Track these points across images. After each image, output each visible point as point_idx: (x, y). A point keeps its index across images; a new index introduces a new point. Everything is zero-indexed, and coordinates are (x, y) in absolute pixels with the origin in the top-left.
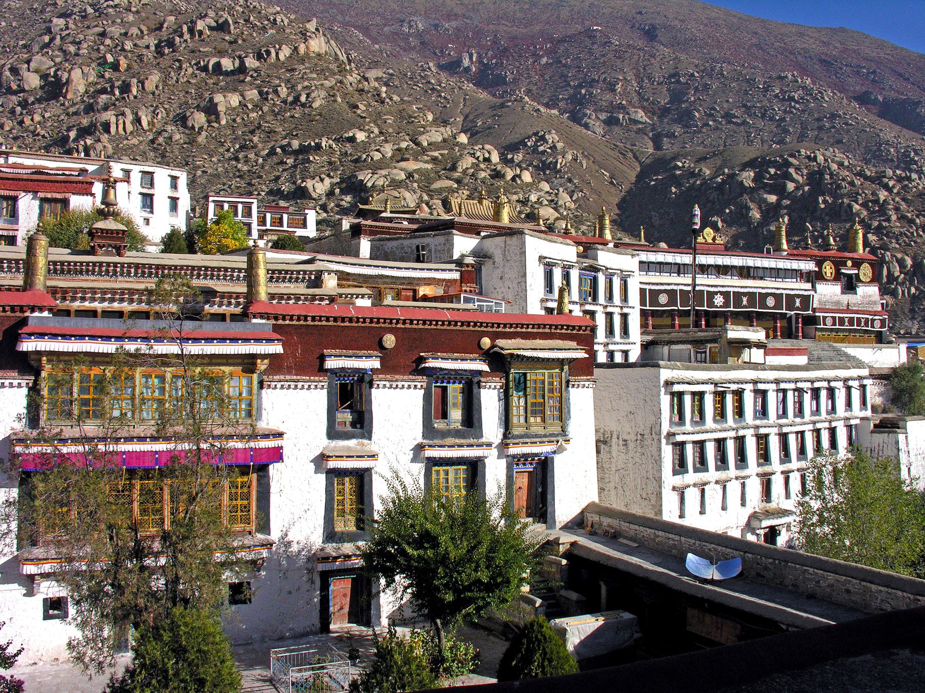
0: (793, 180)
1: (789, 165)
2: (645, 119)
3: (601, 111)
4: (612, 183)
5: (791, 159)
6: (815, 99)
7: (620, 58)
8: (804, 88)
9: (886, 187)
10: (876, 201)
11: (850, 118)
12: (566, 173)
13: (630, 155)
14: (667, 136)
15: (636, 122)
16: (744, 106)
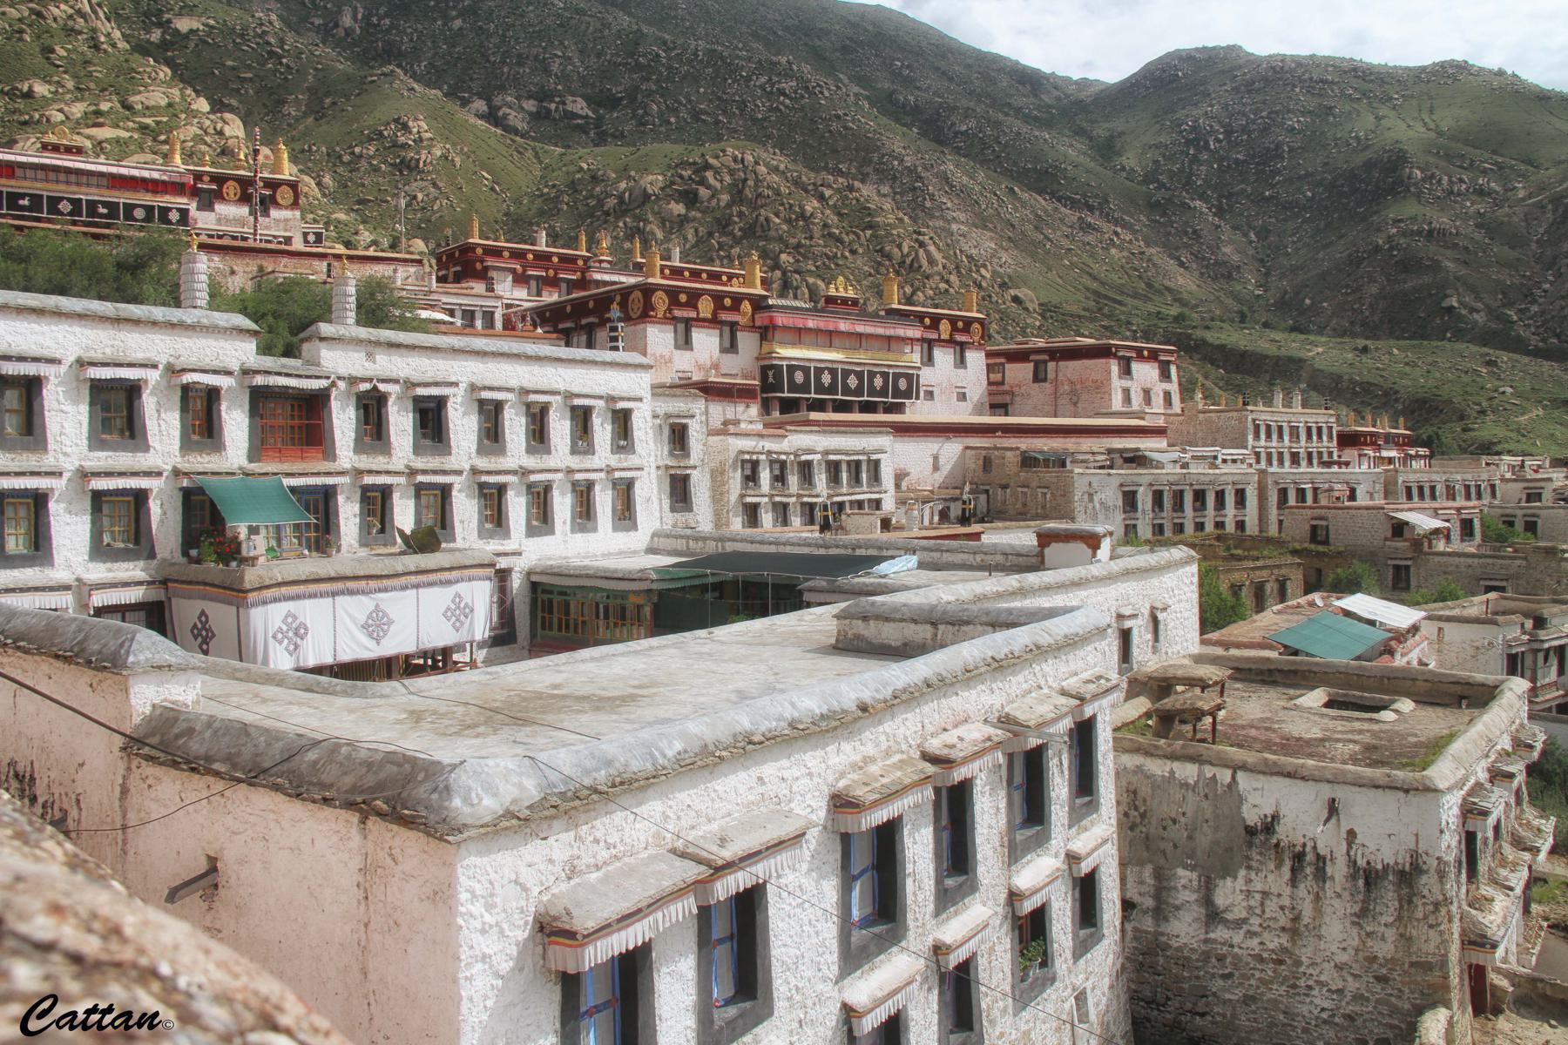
0: (709, 187)
1: (707, 166)
4: (493, 189)
5: (711, 161)
6: (812, 94)
8: (800, 79)
9: (821, 198)
11: (853, 121)
15: (575, 116)
16: (719, 99)
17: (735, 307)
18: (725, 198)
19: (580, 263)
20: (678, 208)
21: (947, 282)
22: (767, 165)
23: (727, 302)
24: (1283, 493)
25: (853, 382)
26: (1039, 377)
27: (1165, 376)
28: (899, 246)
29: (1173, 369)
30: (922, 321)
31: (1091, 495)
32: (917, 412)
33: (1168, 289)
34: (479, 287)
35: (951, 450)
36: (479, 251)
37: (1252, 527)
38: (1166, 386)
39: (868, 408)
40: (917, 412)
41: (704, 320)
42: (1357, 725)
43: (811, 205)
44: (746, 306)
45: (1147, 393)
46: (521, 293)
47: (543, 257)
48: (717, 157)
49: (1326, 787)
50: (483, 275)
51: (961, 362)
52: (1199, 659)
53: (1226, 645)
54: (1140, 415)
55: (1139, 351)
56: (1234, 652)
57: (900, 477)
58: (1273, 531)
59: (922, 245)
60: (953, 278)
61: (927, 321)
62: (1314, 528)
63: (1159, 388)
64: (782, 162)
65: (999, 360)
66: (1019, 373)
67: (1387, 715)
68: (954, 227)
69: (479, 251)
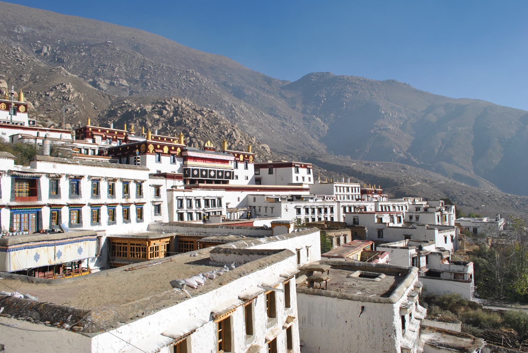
0: (166, 110)
1: (166, 104)
2: (126, 84)
3: (107, 79)
7: (119, 56)
8: (196, 77)
9: (202, 114)
10: (196, 120)
12: (73, 102)
13: (107, 97)
14: (135, 92)
16: (170, 82)
17: (175, 150)
18: (172, 114)
19: (124, 134)
20: (157, 117)
21: (242, 142)
22: (185, 104)
23: (173, 148)
24: (345, 208)
25: (212, 174)
26: (271, 172)
27: (309, 173)
28: (227, 130)
29: (311, 170)
30: (234, 155)
31: (287, 210)
32: (232, 183)
33: (309, 145)
34: (90, 141)
35: (243, 195)
36: (90, 129)
37: (336, 220)
38: (309, 176)
39: (217, 182)
40: (232, 183)
41: (166, 154)
42: (371, 282)
43: (199, 117)
44: (179, 150)
45: (303, 178)
46: (103, 143)
47: (112, 132)
48: (169, 101)
49: (360, 302)
50: (92, 137)
51: (246, 168)
52: (321, 263)
53: (329, 257)
54: (301, 184)
55: (301, 165)
56: (332, 260)
57: (227, 204)
58: (342, 220)
59: (234, 130)
60: (244, 141)
61: (236, 155)
62: (354, 219)
63: (307, 177)
64: (190, 103)
65: (257, 167)
66: (264, 172)
67: (378, 279)
68: (244, 124)
69: (90, 129)
